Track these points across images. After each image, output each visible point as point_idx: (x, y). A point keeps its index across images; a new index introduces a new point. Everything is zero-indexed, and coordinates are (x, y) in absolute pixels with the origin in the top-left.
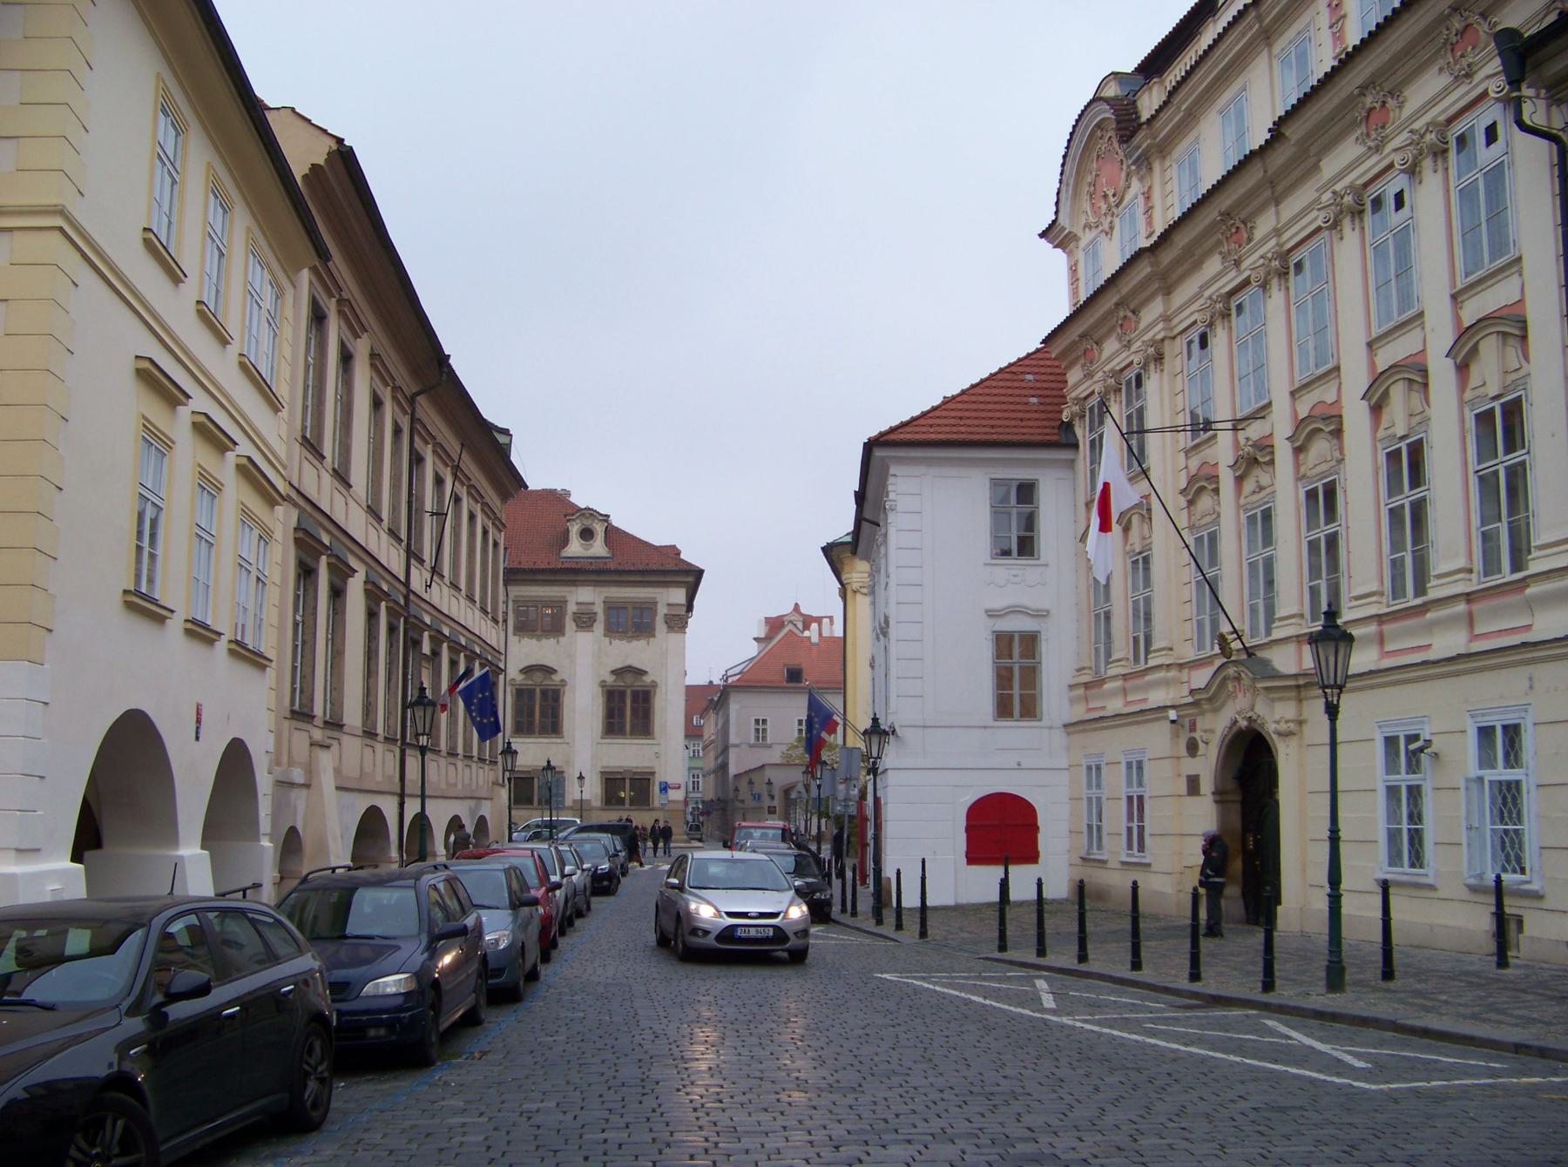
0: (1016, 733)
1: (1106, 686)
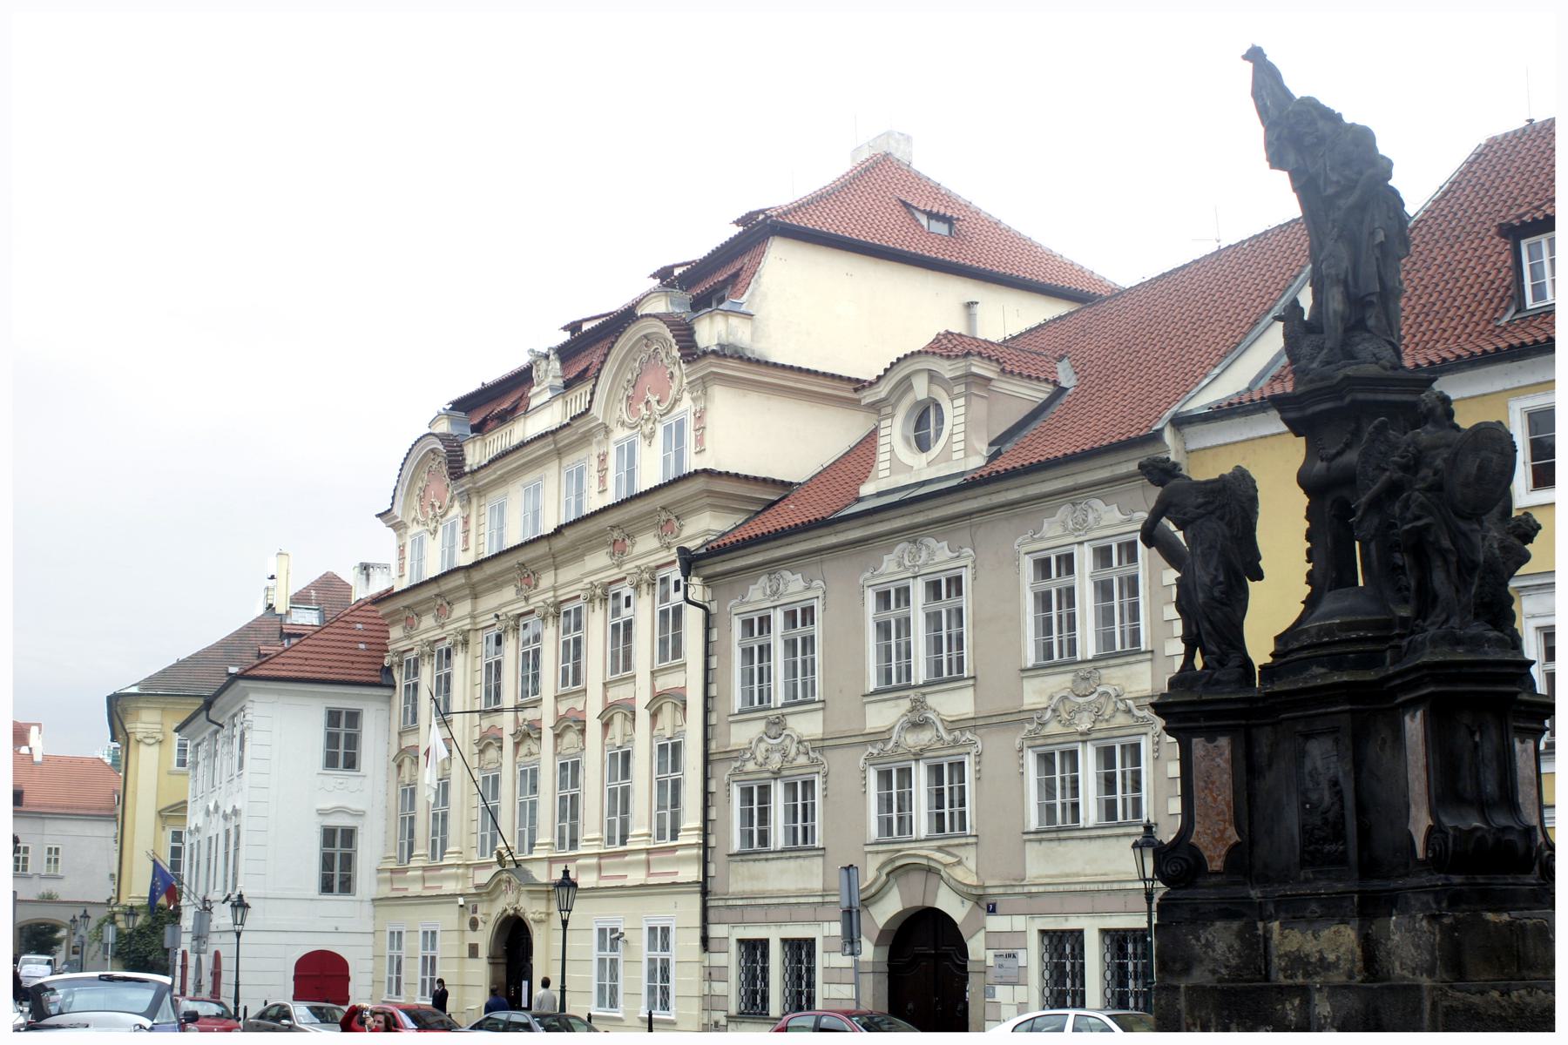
0: (336, 903)
1: (409, 873)
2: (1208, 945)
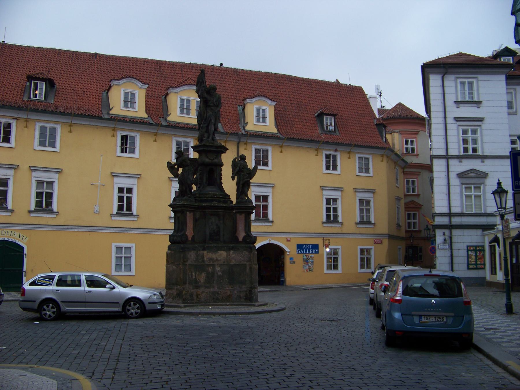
2: (191, 256)
